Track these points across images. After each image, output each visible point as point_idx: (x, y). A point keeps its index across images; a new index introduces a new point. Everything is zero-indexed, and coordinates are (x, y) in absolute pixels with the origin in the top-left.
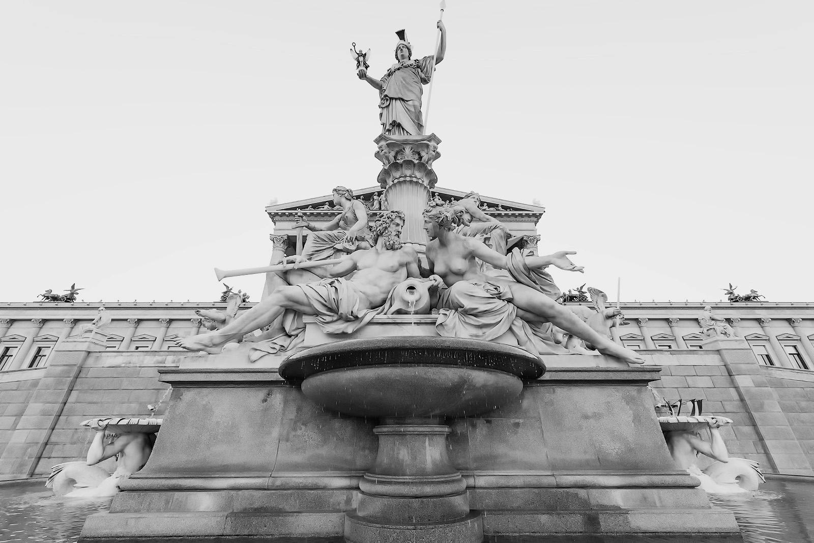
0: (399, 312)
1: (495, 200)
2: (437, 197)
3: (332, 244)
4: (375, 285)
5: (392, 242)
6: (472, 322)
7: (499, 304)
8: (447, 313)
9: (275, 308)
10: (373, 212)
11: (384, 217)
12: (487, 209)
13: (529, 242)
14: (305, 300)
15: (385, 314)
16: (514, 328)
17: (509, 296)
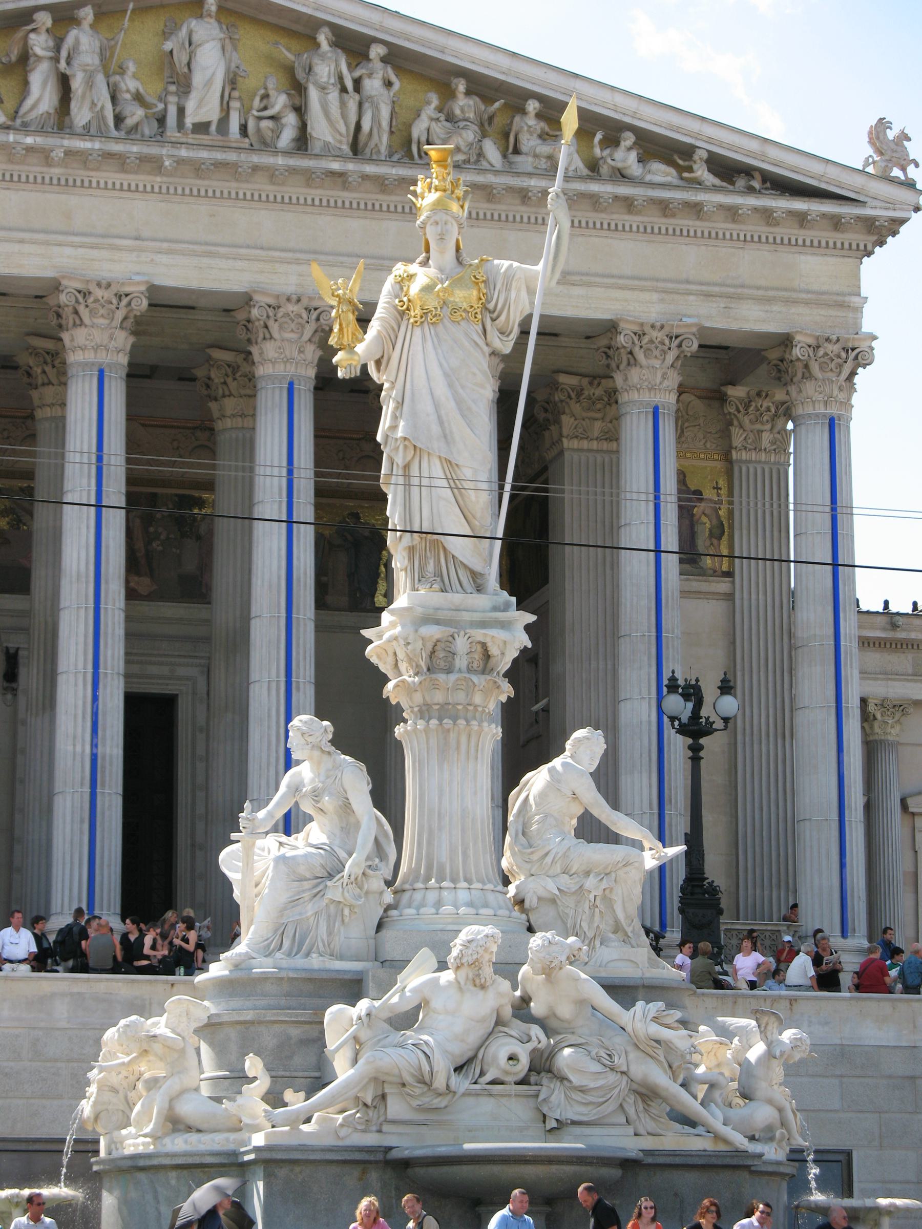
0: (493, 1082)
1: (676, 120)
2: (377, 65)
3: (319, 884)
4: (462, 1041)
5: (483, 981)
6: (579, 1099)
7: (612, 1078)
8: (552, 1086)
9: (367, 1080)
10: (29, 140)
11: (474, 944)
12: (635, 169)
13: (815, 368)
14: (396, 1071)
15: (475, 1083)
16: (625, 1106)
17: (624, 1069)
